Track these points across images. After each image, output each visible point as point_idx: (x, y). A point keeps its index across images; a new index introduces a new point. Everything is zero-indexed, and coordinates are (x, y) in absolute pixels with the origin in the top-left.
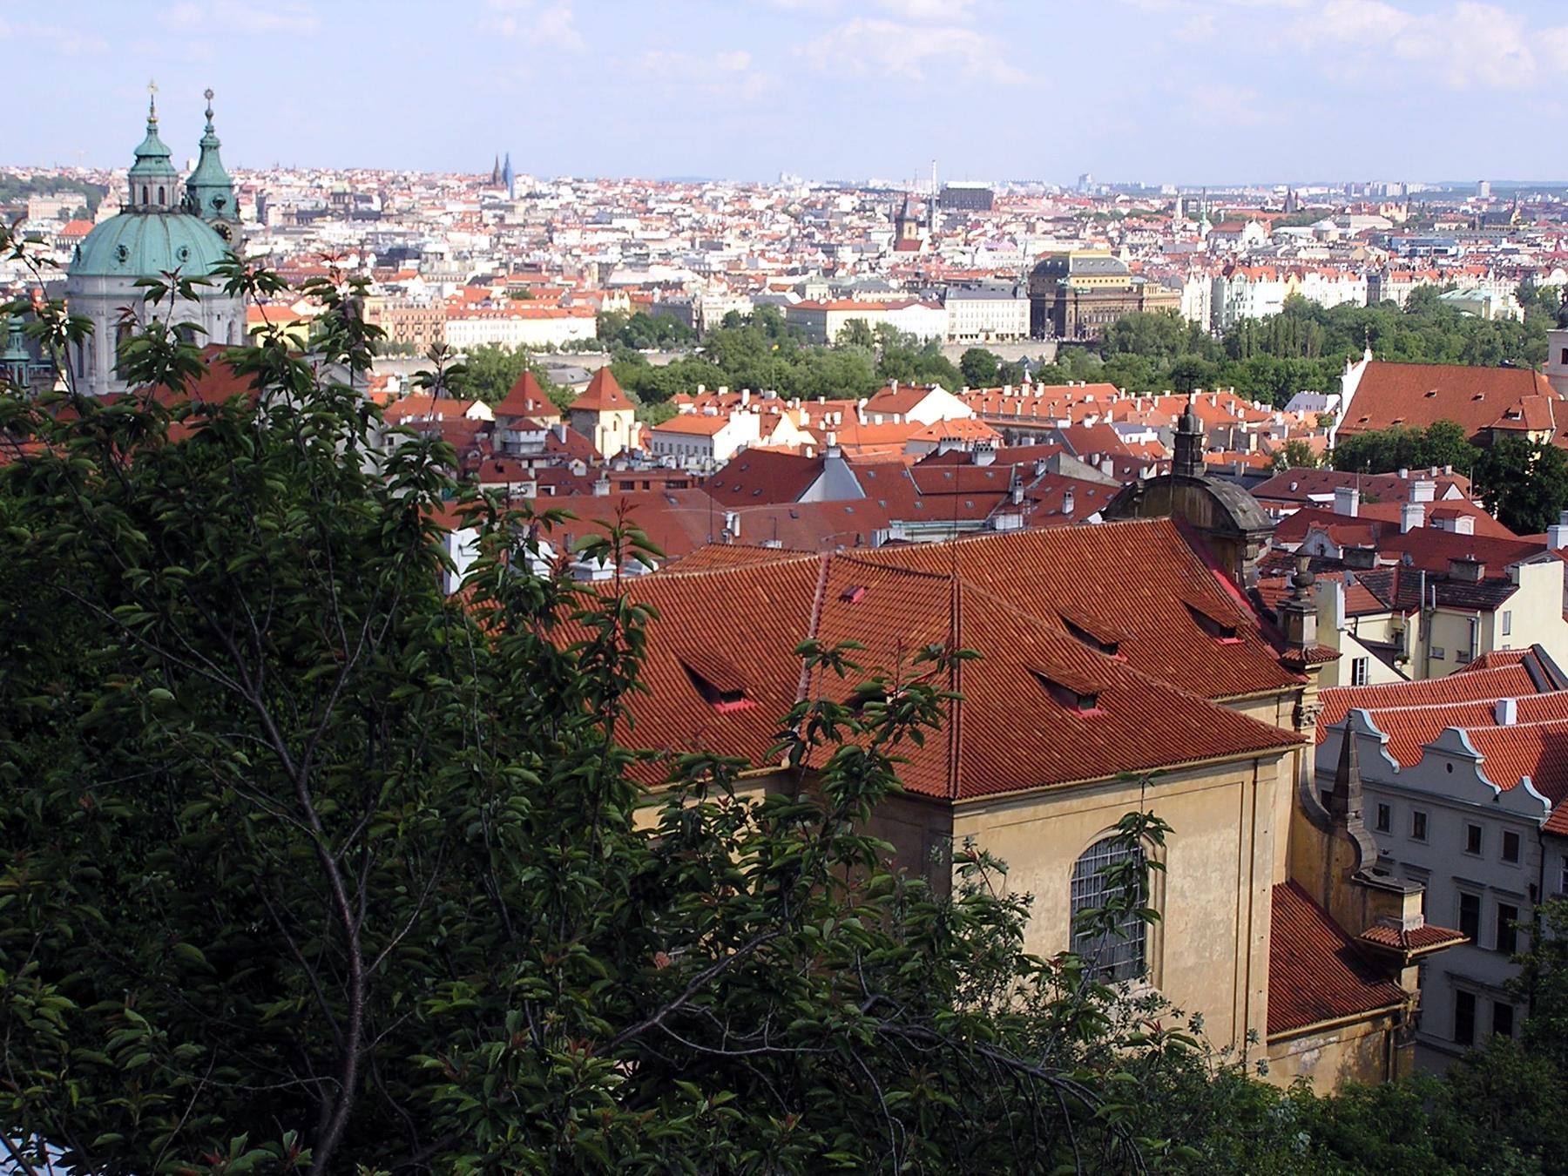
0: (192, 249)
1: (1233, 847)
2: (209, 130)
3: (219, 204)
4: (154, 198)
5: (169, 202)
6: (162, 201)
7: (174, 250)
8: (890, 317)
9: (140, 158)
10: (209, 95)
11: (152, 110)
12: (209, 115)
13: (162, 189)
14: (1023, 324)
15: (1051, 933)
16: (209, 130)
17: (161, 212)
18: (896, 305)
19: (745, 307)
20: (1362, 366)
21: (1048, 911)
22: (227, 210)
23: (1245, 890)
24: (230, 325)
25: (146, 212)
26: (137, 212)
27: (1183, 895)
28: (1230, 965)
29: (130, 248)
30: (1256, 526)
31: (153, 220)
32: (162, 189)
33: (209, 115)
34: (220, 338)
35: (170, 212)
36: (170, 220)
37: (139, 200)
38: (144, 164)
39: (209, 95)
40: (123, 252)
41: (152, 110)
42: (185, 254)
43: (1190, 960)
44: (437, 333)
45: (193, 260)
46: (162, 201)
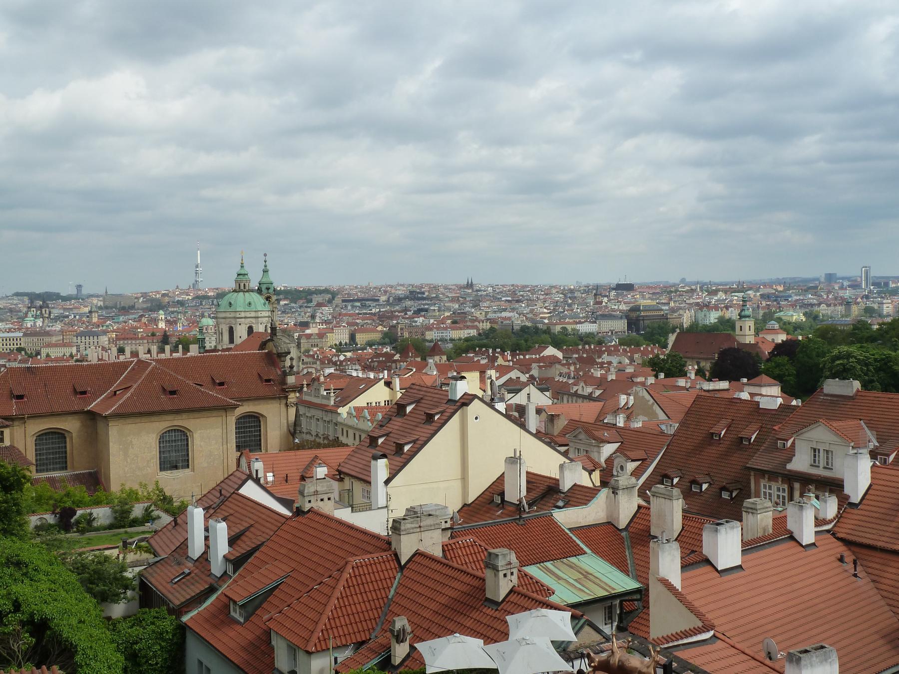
0: (253, 303)
1: (220, 434)
2: (266, 266)
3: (268, 289)
4: (242, 287)
5: (247, 288)
6: (245, 288)
7: (246, 303)
8: (578, 327)
9: (239, 275)
10: (265, 255)
11: (242, 260)
12: (265, 261)
13: (244, 284)
14: (624, 328)
15: (149, 454)
16: (266, 266)
17: (244, 292)
18: (580, 323)
19: (529, 324)
20: (675, 334)
21: (148, 448)
22: (271, 291)
23: (225, 446)
24: (266, 326)
25: (239, 292)
26: (237, 292)
27: (201, 446)
28: (221, 467)
29: (232, 302)
30: (283, 351)
31: (241, 294)
32: (244, 284)
33: (265, 261)
34: (261, 329)
35: (247, 291)
36: (247, 294)
37: (238, 288)
38: (240, 277)
39: (265, 255)
40: (230, 304)
41: (242, 260)
42: (250, 304)
43: (206, 465)
44: (423, 335)
45: (253, 306)
46: (245, 288)
